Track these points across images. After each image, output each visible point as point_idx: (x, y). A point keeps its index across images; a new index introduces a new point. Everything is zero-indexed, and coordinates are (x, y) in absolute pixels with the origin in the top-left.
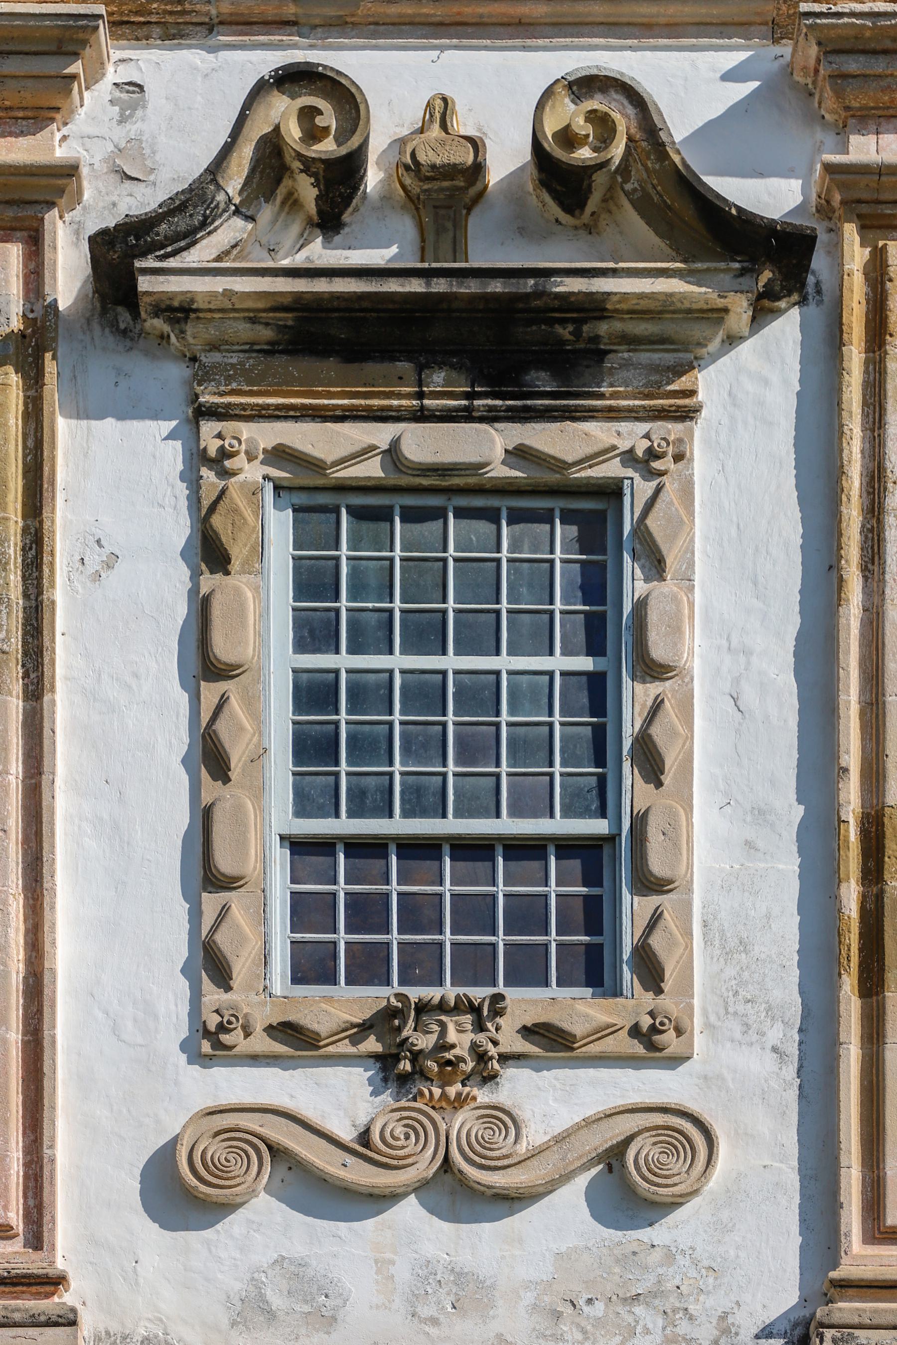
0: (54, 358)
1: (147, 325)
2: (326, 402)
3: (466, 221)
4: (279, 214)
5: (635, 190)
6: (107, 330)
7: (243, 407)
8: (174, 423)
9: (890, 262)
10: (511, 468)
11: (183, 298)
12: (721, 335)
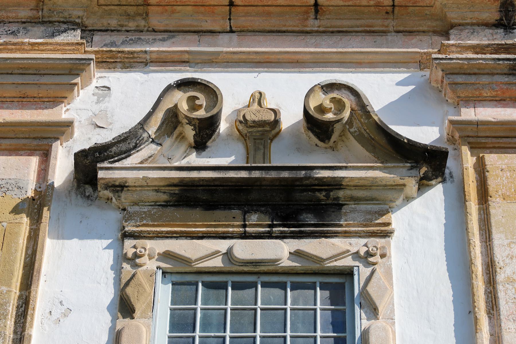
0: (48, 210)
1: (101, 194)
2: (194, 229)
3: (270, 147)
4: (174, 142)
5: (356, 131)
6: (79, 196)
7: (149, 232)
8: (110, 241)
9: (487, 163)
10: (293, 261)
11: (121, 181)
12: (402, 197)
